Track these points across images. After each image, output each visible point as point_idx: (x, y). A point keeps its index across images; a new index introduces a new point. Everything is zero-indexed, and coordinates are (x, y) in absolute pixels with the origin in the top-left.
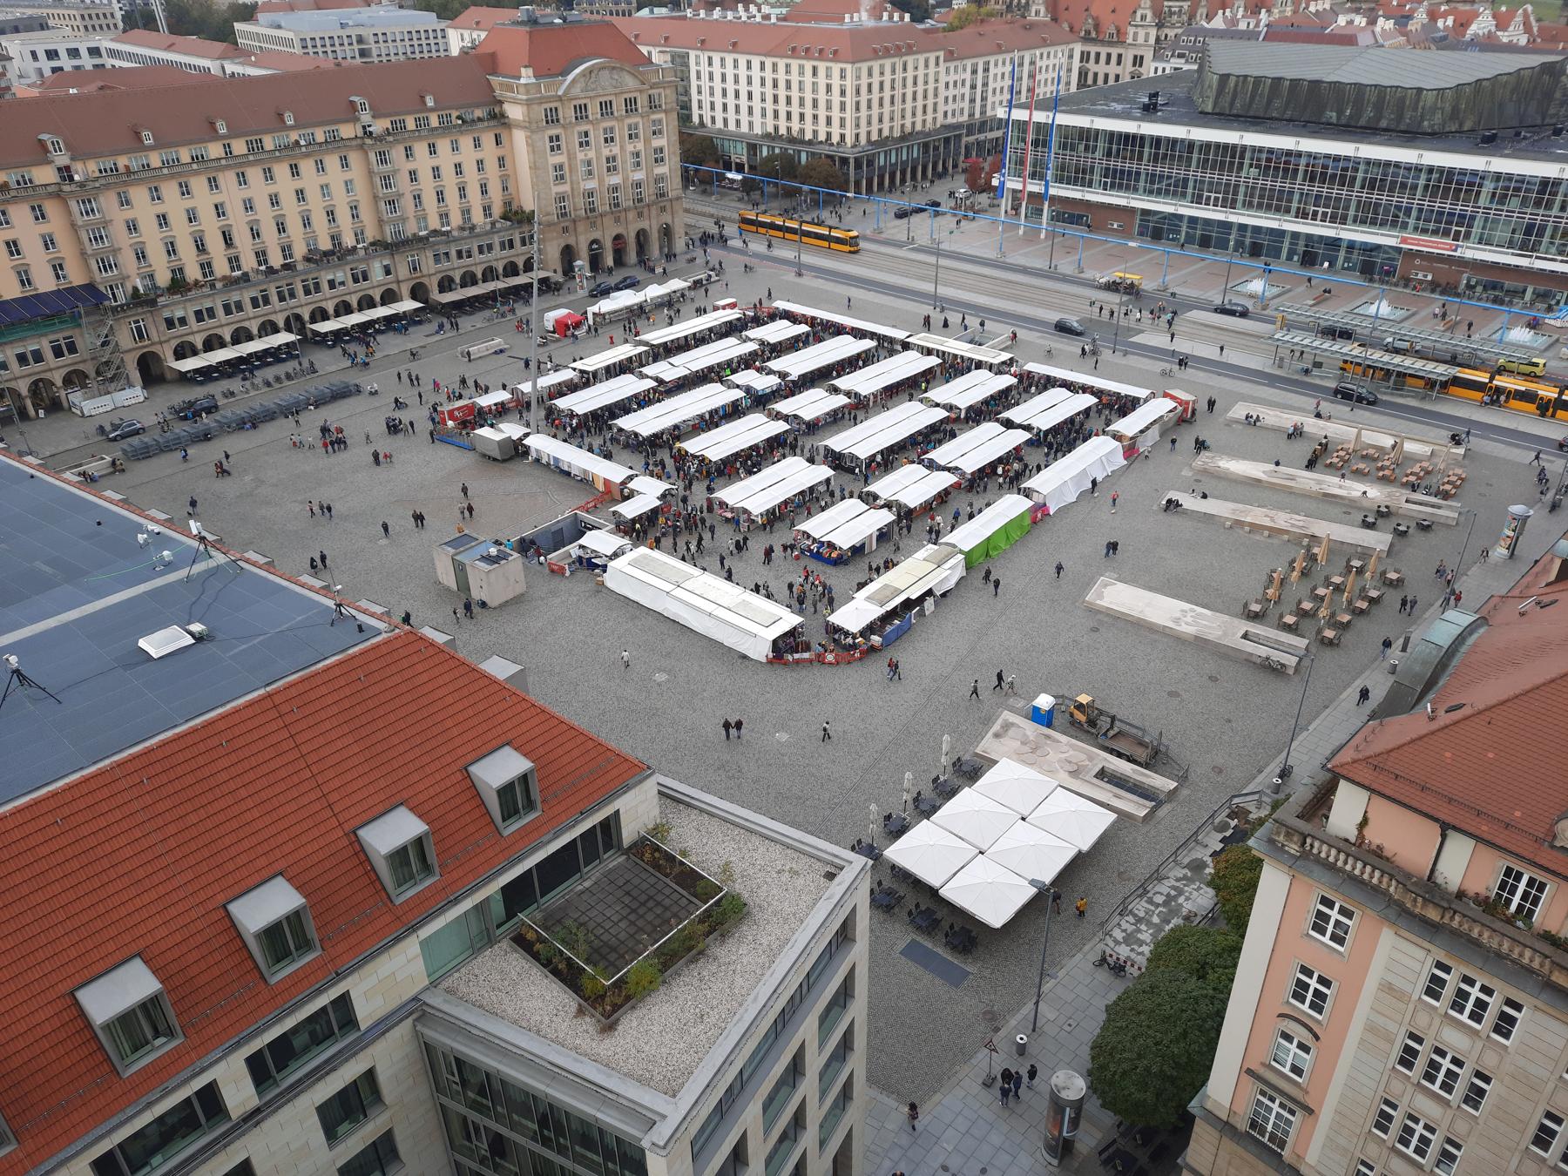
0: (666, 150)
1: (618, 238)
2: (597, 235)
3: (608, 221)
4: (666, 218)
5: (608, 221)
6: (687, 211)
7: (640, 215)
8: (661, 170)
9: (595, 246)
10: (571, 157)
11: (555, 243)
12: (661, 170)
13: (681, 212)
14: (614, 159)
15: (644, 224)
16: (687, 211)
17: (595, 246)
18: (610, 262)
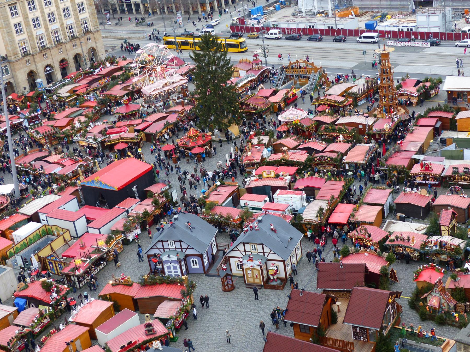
0: (85, 4)
1: (62, 61)
2: (49, 62)
3: (54, 52)
4: (92, 44)
5: (54, 52)
6: (103, 37)
7: (74, 45)
8: (82, 16)
9: (48, 69)
10: (26, 17)
11: (22, 70)
12: (82, 16)
13: (101, 40)
14: (53, 14)
15: (78, 50)
16: (103, 37)
17: (48, 69)
18: (59, 76)
